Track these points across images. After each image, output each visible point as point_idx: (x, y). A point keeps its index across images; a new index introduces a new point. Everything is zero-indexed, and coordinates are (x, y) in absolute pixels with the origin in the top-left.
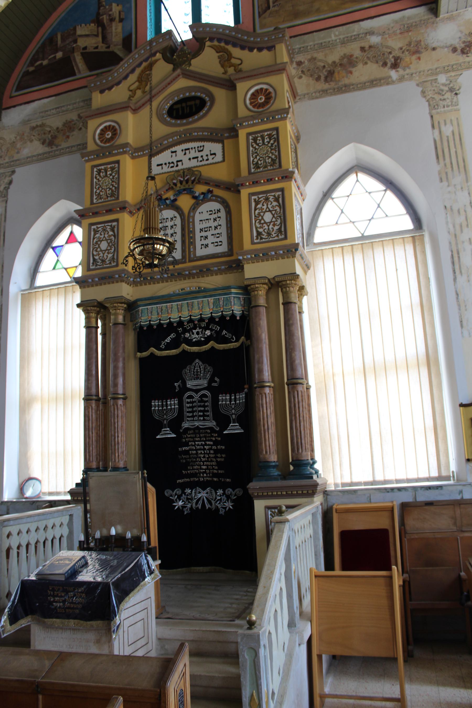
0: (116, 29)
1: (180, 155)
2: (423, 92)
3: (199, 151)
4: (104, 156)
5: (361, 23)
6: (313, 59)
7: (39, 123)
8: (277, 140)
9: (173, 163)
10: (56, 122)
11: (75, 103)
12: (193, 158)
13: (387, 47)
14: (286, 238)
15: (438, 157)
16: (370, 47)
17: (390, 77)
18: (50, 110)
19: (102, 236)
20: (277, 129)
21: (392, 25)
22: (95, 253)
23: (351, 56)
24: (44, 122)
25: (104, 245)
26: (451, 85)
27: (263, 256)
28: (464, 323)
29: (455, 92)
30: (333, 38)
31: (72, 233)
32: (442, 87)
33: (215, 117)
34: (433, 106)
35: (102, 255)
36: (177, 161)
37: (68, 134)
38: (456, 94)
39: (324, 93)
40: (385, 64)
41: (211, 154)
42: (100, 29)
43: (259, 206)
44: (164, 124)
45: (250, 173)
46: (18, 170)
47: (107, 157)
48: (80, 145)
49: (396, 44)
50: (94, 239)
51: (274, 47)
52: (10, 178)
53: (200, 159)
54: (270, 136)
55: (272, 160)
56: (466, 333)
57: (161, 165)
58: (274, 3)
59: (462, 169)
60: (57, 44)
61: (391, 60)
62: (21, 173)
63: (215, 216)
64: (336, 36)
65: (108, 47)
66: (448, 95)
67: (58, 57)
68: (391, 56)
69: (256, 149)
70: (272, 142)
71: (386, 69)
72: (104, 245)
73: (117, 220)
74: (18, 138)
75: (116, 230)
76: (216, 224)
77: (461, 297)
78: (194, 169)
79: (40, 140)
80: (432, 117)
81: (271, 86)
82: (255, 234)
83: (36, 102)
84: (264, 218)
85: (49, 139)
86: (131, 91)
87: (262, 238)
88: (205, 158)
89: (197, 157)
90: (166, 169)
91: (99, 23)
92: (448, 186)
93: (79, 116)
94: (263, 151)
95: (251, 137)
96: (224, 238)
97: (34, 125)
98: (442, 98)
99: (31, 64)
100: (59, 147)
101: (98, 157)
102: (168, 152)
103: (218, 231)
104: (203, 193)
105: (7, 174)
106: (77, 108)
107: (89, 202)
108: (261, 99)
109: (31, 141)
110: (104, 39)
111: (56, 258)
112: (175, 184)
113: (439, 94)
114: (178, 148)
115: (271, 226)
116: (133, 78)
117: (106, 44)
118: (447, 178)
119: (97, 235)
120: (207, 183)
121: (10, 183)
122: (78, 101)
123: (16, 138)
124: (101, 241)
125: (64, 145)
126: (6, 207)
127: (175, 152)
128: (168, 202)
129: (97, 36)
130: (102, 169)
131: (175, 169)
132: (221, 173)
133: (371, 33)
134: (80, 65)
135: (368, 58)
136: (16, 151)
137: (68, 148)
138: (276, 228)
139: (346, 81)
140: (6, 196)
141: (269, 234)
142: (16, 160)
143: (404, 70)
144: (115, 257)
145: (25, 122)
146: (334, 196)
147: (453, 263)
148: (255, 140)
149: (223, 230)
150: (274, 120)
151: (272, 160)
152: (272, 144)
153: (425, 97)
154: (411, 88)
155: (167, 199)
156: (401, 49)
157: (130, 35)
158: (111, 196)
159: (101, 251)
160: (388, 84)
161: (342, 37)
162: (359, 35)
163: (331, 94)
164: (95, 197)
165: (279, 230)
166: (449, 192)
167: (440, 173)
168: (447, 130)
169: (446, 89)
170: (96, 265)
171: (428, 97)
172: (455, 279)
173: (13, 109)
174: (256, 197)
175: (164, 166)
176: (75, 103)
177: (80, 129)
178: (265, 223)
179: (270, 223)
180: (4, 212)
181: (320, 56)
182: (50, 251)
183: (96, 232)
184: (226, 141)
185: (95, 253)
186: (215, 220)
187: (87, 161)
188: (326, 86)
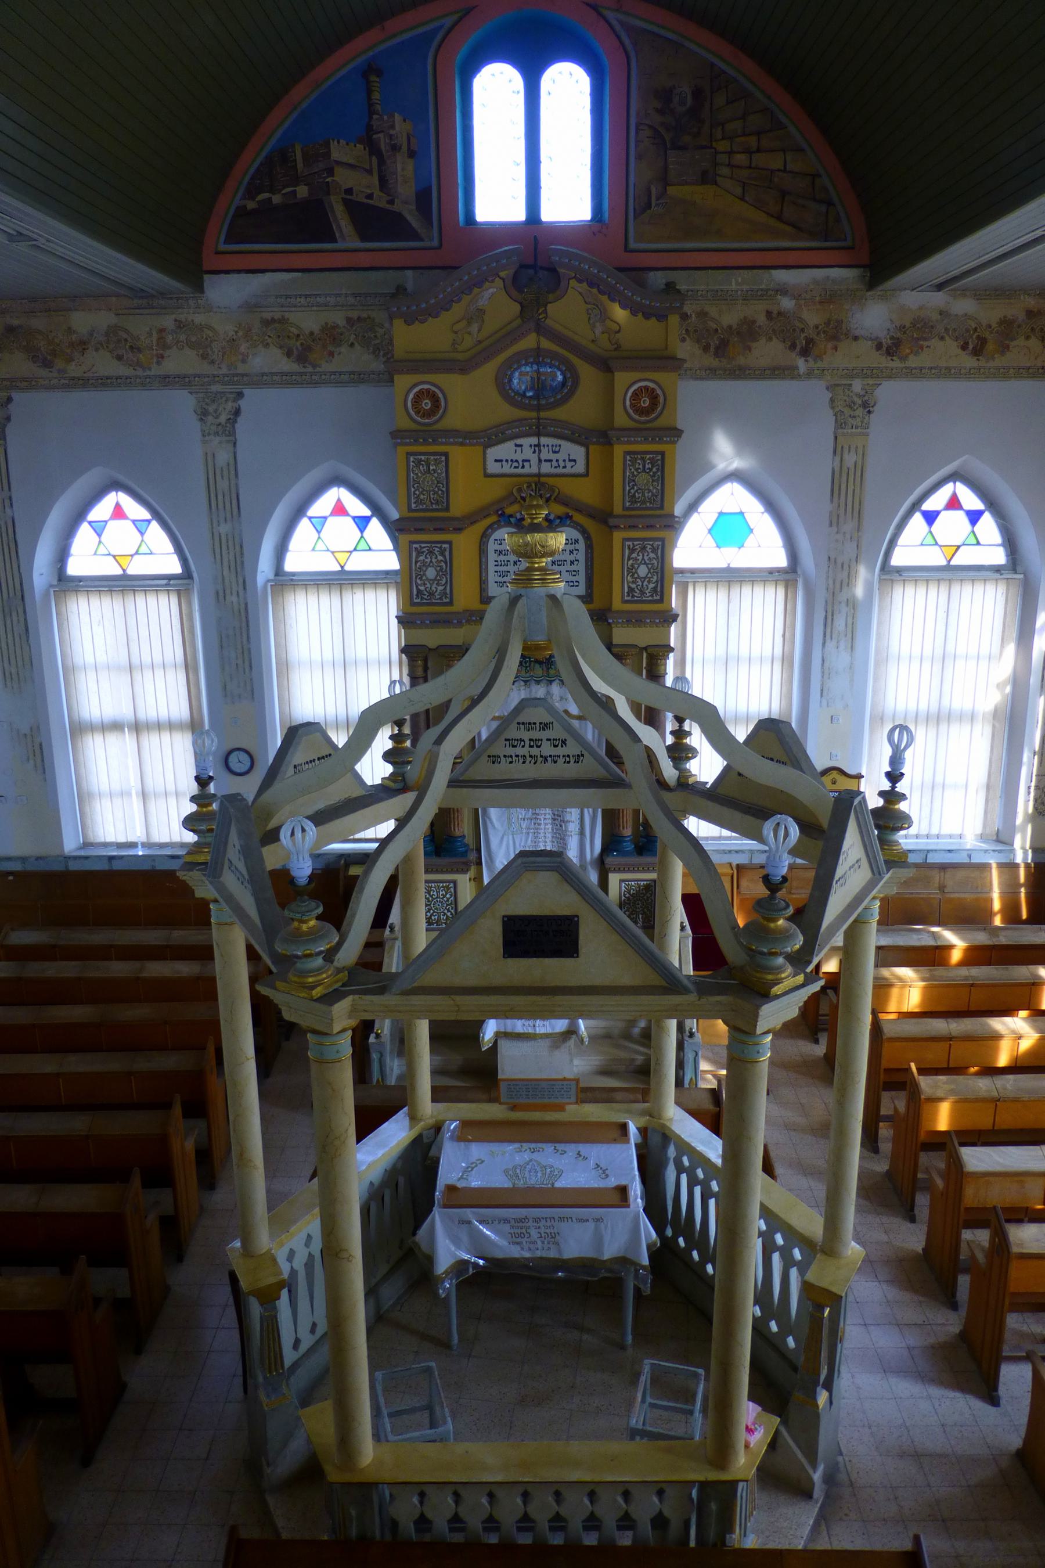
0: (403, 169)
1: (528, 453)
2: (832, 400)
3: (555, 452)
4: (425, 442)
5: (773, 272)
6: (703, 314)
7: (277, 316)
8: (662, 468)
9: (517, 461)
10: (308, 322)
11: (340, 295)
12: (546, 461)
13: (801, 320)
14: (661, 601)
15: (832, 495)
16: (779, 313)
17: (797, 368)
18: (296, 296)
19: (428, 560)
20: (663, 454)
21: (812, 287)
22: (419, 582)
23: (754, 322)
24: (287, 315)
25: (431, 573)
26: (866, 398)
27: (636, 619)
28: (825, 693)
29: (868, 407)
30: (734, 287)
31: (339, 501)
32: (856, 399)
33: (581, 409)
34: (840, 424)
35: (428, 585)
36: (524, 461)
37: (330, 348)
38: (869, 412)
39: (712, 373)
40: (793, 347)
41: (570, 460)
42: (374, 158)
43: (634, 555)
44: (500, 393)
45: (625, 508)
46: (247, 392)
47: (429, 444)
48: (353, 373)
49: (812, 318)
50: (416, 562)
51: (667, 316)
52: (235, 405)
53: (555, 464)
54: (653, 462)
55: (653, 495)
56: (824, 703)
57: (501, 461)
58: (657, 199)
59: (856, 514)
60: (295, 167)
61: (801, 342)
62: (253, 399)
63: (572, 547)
64: (737, 283)
65: (391, 202)
66: (860, 412)
67: (299, 196)
68: (803, 336)
69: (634, 476)
70: (654, 470)
71: (793, 355)
72: (431, 573)
73: (450, 543)
74: (240, 333)
75: (447, 553)
76: (572, 557)
77: (826, 664)
78: (551, 481)
79: (281, 347)
80: (836, 438)
81: (665, 399)
82: (626, 590)
83: (268, 275)
84: (639, 571)
85: (297, 348)
86: (456, 333)
87: (633, 596)
88: (562, 464)
89: (551, 461)
90: (507, 469)
91: (373, 149)
92: (837, 533)
93: (349, 320)
94: (643, 479)
95: (628, 458)
96: (582, 578)
97: (267, 316)
98: (852, 413)
99: (251, 192)
100: (318, 369)
101: (416, 442)
102: (510, 445)
103: (574, 567)
104: (559, 517)
105: (228, 395)
106: (343, 306)
107: (405, 509)
108: (645, 402)
109: (267, 345)
110: (383, 182)
111: (317, 535)
112: (524, 499)
113: (850, 407)
114: (528, 441)
115: (645, 583)
116: (458, 310)
117: (388, 194)
118: (838, 523)
119: (421, 558)
120: (566, 504)
121: (237, 412)
122: (344, 291)
123: (236, 332)
124: (427, 567)
125: (326, 367)
126: (235, 453)
127: (521, 446)
128: (512, 520)
129: (369, 172)
130: (421, 460)
131: (519, 471)
132: (585, 492)
133: (783, 290)
134: (343, 223)
135: (774, 330)
136: (240, 357)
137: (334, 373)
138: (652, 586)
139: (741, 361)
140: (232, 433)
141: (642, 593)
142: (243, 375)
143: (815, 361)
144: (448, 591)
145: (251, 307)
146: (699, 510)
147: (825, 625)
148: (634, 461)
149: (581, 567)
150: (661, 441)
151: (653, 495)
152: (655, 473)
153: (833, 408)
154: (817, 392)
155: (511, 516)
156: (817, 327)
157: (430, 188)
158: (437, 503)
159: (427, 579)
160: (792, 378)
161: (745, 287)
162: (767, 290)
163: (721, 378)
164: (413, 500)
165: (655, 590)
166: (837, 541)
167: (831, 512)
168: (850, 459)
169: (859, 401)
170: (422, 599)
171: (837, 409)
172: (824, 644)
173: (223, 276)
174: (630, 543)
175: (504, 463)
176: (340, 295)
177: (352, 345)
178: (639, 577)
179: (645, 578)
180: (232, 462)
181: (713, 311)
182: (304, 523)
183: (419, 553)
184: (592, 448)
185: (419, 582)
186: (571, 552)
187: (400, 444)
188: (715, 363)
